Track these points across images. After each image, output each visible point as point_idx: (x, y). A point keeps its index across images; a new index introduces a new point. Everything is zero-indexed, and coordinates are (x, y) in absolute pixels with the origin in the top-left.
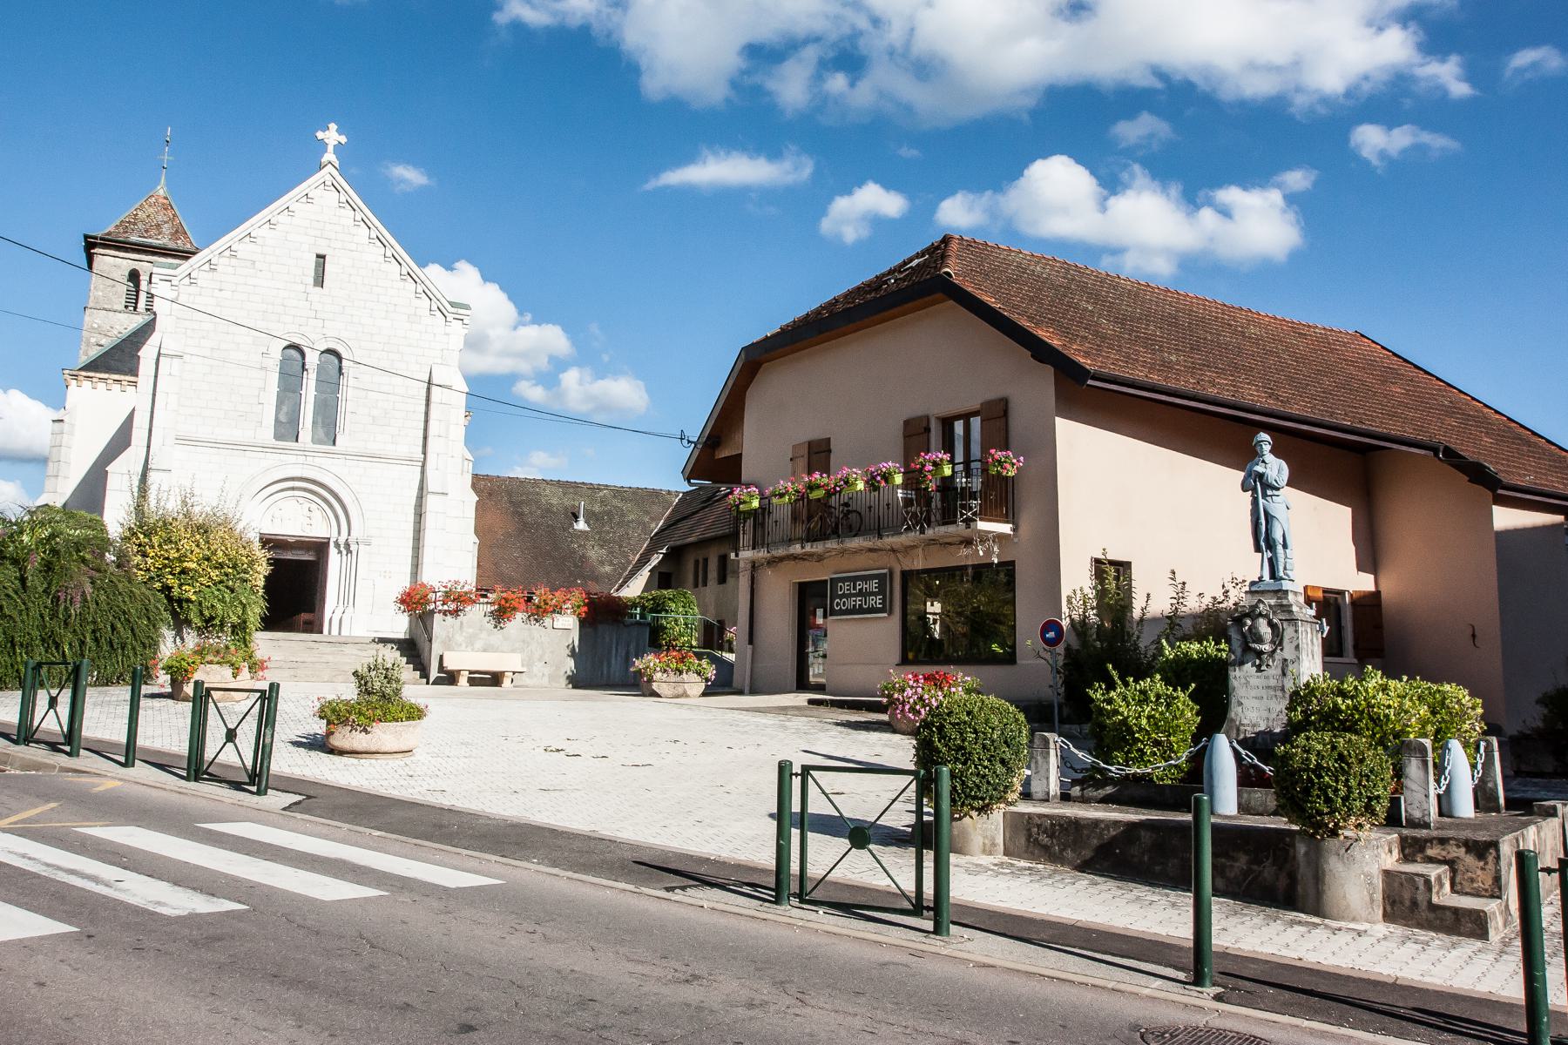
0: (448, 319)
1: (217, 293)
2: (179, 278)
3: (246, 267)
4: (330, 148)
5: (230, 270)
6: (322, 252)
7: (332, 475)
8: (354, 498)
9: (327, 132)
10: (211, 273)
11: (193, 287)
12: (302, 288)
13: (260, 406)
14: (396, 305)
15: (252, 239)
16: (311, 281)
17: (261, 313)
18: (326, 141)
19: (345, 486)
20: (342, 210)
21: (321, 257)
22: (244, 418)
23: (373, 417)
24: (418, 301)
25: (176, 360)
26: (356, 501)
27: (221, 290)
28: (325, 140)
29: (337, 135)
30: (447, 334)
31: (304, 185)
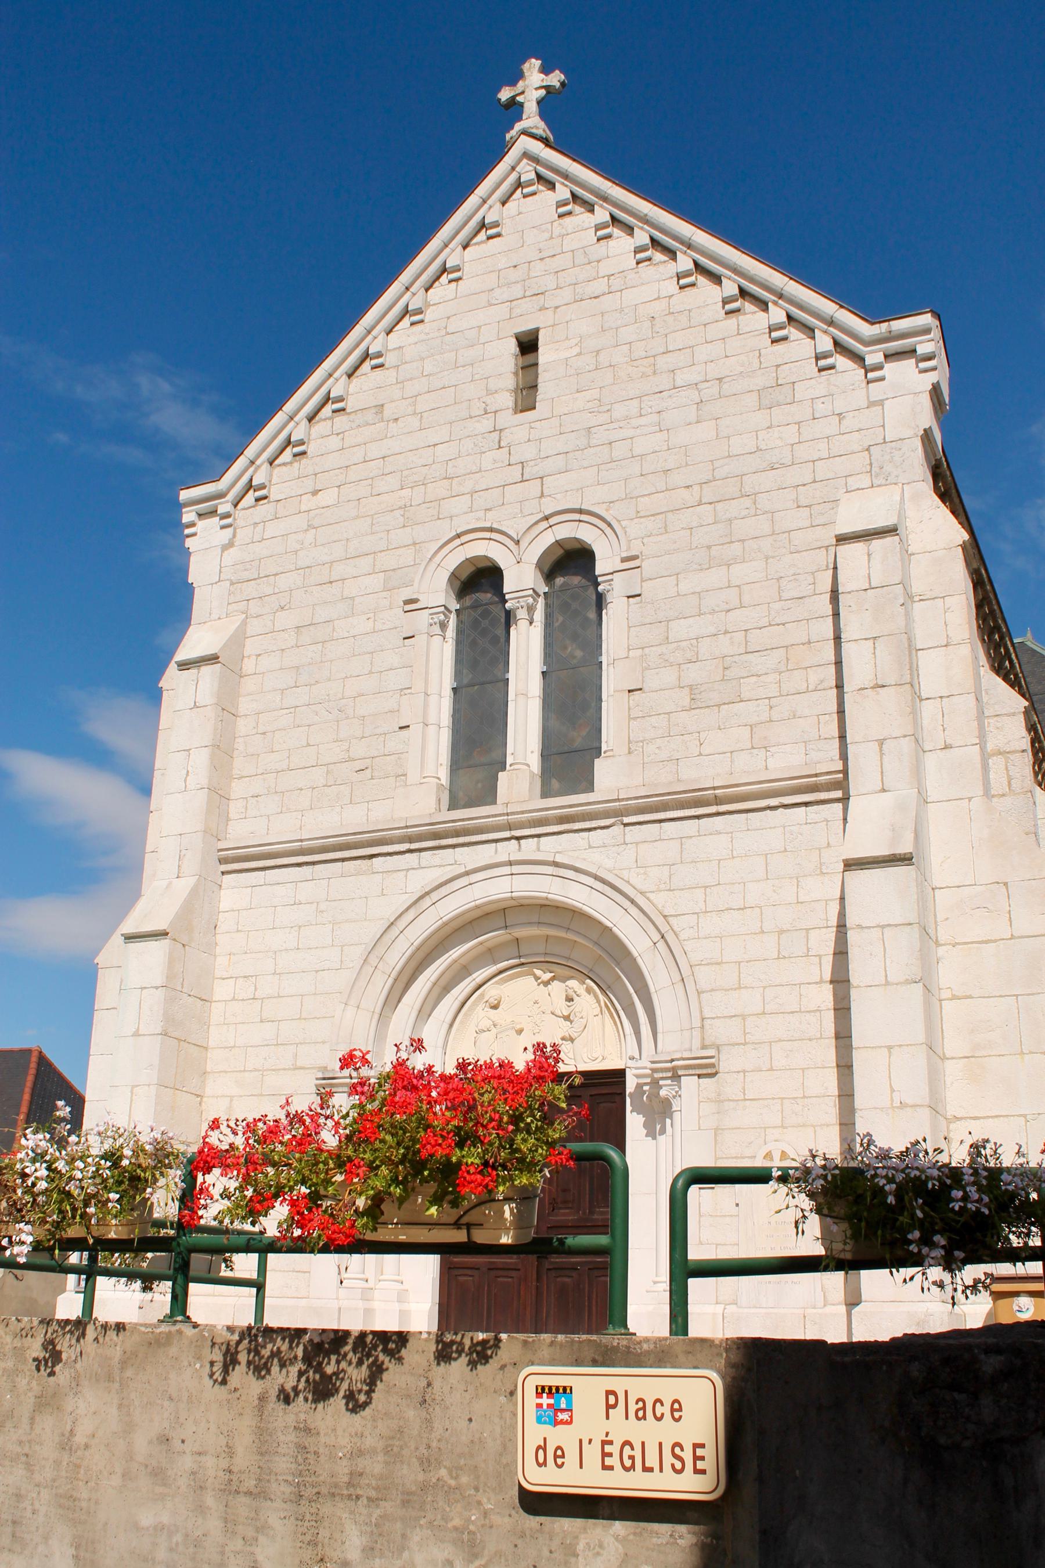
0: (869, 360)
1: (308, 502)
2: (230, 496)
3: (368, 424)
4: (531, 107)
5: (334, 442)
6: (525, 326)
7: (589, 881)
8: (656, 937)
9: (521, 83)
10: (296, 465)
11: (264, 507)
12: (487, 424)
13: (404, 732)
14: (720, 379)
15: (374, 362)
16: (507, 400)
17: (398, 513)
18: (519, 99)
19: (627, 904)
20: (567, 220)
21: (528, 345)
22: (368, 771)
23: (691, 687)
24: (780, 347)
25: (206, 670)
26: (661, 945)
27: (315, 493)
28: (518, 98)
29: (542, 76)
30: (881, 403)
31: (473, 200)
